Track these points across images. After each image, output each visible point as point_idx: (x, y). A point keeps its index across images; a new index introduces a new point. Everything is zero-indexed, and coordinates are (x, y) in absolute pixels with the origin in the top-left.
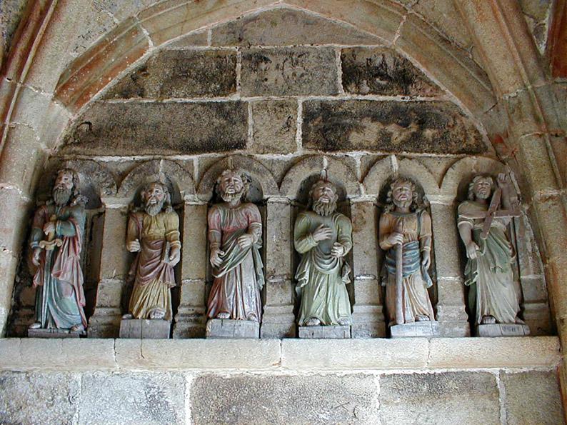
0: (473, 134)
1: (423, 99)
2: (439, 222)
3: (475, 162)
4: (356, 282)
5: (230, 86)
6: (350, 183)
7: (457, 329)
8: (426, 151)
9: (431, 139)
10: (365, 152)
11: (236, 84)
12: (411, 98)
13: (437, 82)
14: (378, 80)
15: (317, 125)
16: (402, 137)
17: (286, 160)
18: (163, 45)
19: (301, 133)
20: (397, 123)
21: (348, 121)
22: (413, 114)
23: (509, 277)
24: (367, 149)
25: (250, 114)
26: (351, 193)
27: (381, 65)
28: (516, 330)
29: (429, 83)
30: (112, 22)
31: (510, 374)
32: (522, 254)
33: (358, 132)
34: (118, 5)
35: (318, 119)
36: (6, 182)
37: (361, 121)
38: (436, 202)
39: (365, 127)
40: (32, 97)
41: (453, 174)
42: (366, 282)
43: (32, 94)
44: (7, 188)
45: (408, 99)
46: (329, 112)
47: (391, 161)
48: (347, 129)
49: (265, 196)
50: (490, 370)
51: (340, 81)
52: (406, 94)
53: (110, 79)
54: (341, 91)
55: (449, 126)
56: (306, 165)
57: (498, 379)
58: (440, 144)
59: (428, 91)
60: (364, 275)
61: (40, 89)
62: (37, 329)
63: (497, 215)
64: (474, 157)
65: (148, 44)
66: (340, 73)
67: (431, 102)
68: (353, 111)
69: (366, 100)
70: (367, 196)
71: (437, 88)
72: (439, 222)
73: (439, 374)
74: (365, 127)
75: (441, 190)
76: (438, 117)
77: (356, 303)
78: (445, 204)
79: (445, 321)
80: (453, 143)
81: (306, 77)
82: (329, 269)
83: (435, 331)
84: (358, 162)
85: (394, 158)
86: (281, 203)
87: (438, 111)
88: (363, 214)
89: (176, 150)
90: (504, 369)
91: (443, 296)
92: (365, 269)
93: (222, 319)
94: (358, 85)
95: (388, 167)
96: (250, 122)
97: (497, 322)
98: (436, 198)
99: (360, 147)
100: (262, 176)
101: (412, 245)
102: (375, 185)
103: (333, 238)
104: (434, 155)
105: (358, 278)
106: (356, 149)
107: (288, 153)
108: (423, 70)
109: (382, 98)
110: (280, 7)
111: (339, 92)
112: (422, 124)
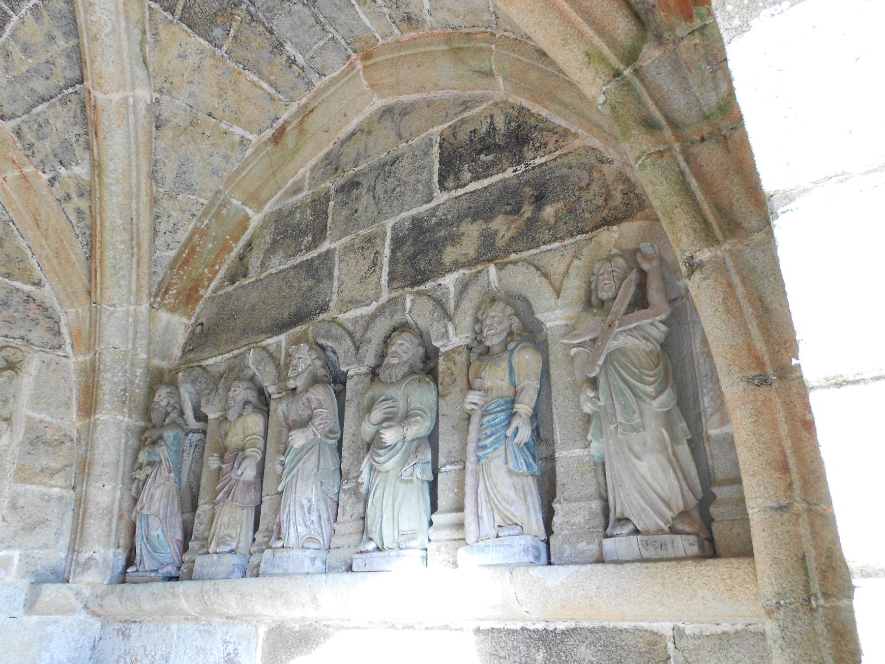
0: (621, 187)
1: (543, 160)
2: (559, 356)
3: (616, 235)
4: (440, 476)
5: (320, 234)
6: (435, 324)
7: (582, 546)
8: (544, 243)
9: (552, 221)
10: (461, 271)
11: (326, 229)
12: (527, 165)
13: (564, 124)
14: (482, 157)
15: (406, 252)
16: (510, 234)
17: (370, 313)
18: (267, 209)
19: (387, 271)
20: (506, 213)
21: (442, 233)
22: (527, 189)
23: (649, 441)
24: (463, 266)
25: (337, 262)
26: (436, 340)
27: (488, 133)
28: (669, 546)
29: (553, 130)
30: (199, 204)
31: (694, 637)
32: (710, 386)
33: (453, 246)
34: (194, 184)
35: (408, 244)
36: (100, 412)
37: (458, 227)
38: (556, 323)
39: (463, 234)
40: (109, 316)
41: (578, 267)
42: (453, 475)
43: (107, 313)
44: (102, 418)
45: (521, 168)
46: (421, 228)
47: (488, 276)
48: (438, 246)
49: (344, 369)
50: (655, 626)
51: (436, 178)
52: (519, 163)
53: (217, 267)
54: (437, 192)
55: (581, 189)
56: (387, 314)
57: (671, 645)
58: (566, 223)
59: (551, 146)
60: (452, 463)
61: (113, 305)
62: (133, 572)
63: (620, 325)
64: (615, 228)
65: (246, 215)
66: (436, 167)
67: (555, 160)
68: (449, 217)
69: (467, 193)
70: (457, 339)
71: (566, 133)
72: (559, 356)
73: (563, 632)
74: (463, 234)
75: (559, 301)
76: (563, 179)
77: (439, 509)
78: (568, 323)
79: (565, 532)
80: (587, 215)
81: (398, 189)
82: (384, 463)
83: (522, 553)
84: (452, 289)
85: (492, 269)
86: (360, 374)
87: (565, 171)
88: (453, 368)
89: (266, 333)
90: (681, 625)
91: (563, 485)
92: (453, 454)
93: (275, 548)
94: (458, 173)
95: (484, 286)
96: (336, 273)
97: (636, 532)
98: (553, 317)
99: (457, 265)
100: (340, 343)
101: (494, 406)
102: (467, 319)
103: (400, 414)
104: (556, 245)
105: (443, 469)
106: (450, 271)
107: (372, 302)
108: (544, 113)
109: (486, 182)
110: (376, 108)
111: (435, 194)
112: (539, 200)
